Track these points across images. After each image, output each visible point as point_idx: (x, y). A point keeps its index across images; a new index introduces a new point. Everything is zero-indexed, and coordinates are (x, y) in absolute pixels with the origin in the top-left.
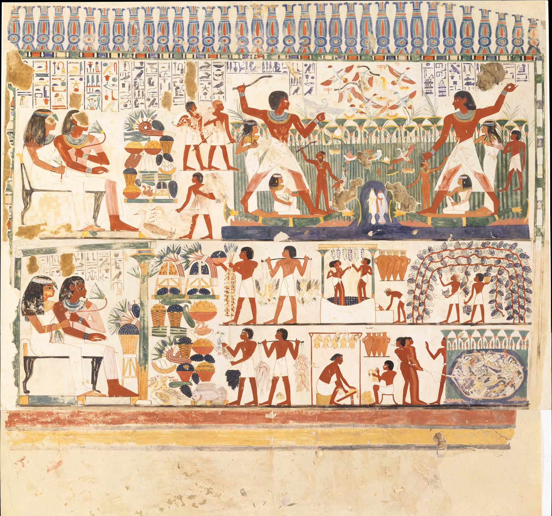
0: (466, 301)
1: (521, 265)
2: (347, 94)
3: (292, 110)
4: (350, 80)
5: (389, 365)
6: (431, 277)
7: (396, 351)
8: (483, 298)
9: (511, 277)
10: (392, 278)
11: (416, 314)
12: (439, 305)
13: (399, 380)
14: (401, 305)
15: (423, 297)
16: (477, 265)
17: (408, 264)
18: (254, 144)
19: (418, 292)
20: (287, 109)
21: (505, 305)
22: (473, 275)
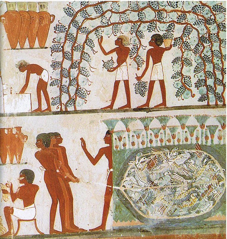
0: (140, 75)
1: (215, 21)
5: (27, 176)
6: (85, 42)
7: (37, 155)
8: (165, 69)
9: (202, 40)
10: (27, 44)
11: (65, 98)
12: (97, 82)
13: (43, 198)
14: (42, 86)
15: (74, 72)
16: (151, 22)
17: (52, 22)
19: (67, 64)
21: (194, 80)
22: (147, 36)
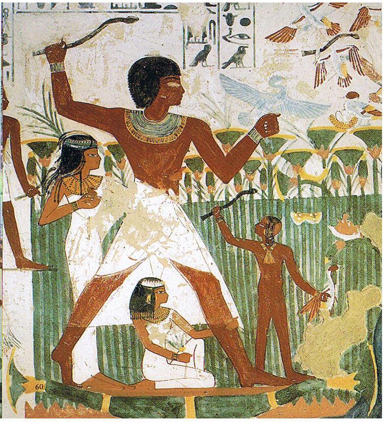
2: (336, 64)
3: (188, 107)
4: (345, 29)
18: (90, 199)
20: (178, 103)
